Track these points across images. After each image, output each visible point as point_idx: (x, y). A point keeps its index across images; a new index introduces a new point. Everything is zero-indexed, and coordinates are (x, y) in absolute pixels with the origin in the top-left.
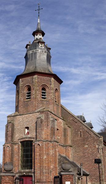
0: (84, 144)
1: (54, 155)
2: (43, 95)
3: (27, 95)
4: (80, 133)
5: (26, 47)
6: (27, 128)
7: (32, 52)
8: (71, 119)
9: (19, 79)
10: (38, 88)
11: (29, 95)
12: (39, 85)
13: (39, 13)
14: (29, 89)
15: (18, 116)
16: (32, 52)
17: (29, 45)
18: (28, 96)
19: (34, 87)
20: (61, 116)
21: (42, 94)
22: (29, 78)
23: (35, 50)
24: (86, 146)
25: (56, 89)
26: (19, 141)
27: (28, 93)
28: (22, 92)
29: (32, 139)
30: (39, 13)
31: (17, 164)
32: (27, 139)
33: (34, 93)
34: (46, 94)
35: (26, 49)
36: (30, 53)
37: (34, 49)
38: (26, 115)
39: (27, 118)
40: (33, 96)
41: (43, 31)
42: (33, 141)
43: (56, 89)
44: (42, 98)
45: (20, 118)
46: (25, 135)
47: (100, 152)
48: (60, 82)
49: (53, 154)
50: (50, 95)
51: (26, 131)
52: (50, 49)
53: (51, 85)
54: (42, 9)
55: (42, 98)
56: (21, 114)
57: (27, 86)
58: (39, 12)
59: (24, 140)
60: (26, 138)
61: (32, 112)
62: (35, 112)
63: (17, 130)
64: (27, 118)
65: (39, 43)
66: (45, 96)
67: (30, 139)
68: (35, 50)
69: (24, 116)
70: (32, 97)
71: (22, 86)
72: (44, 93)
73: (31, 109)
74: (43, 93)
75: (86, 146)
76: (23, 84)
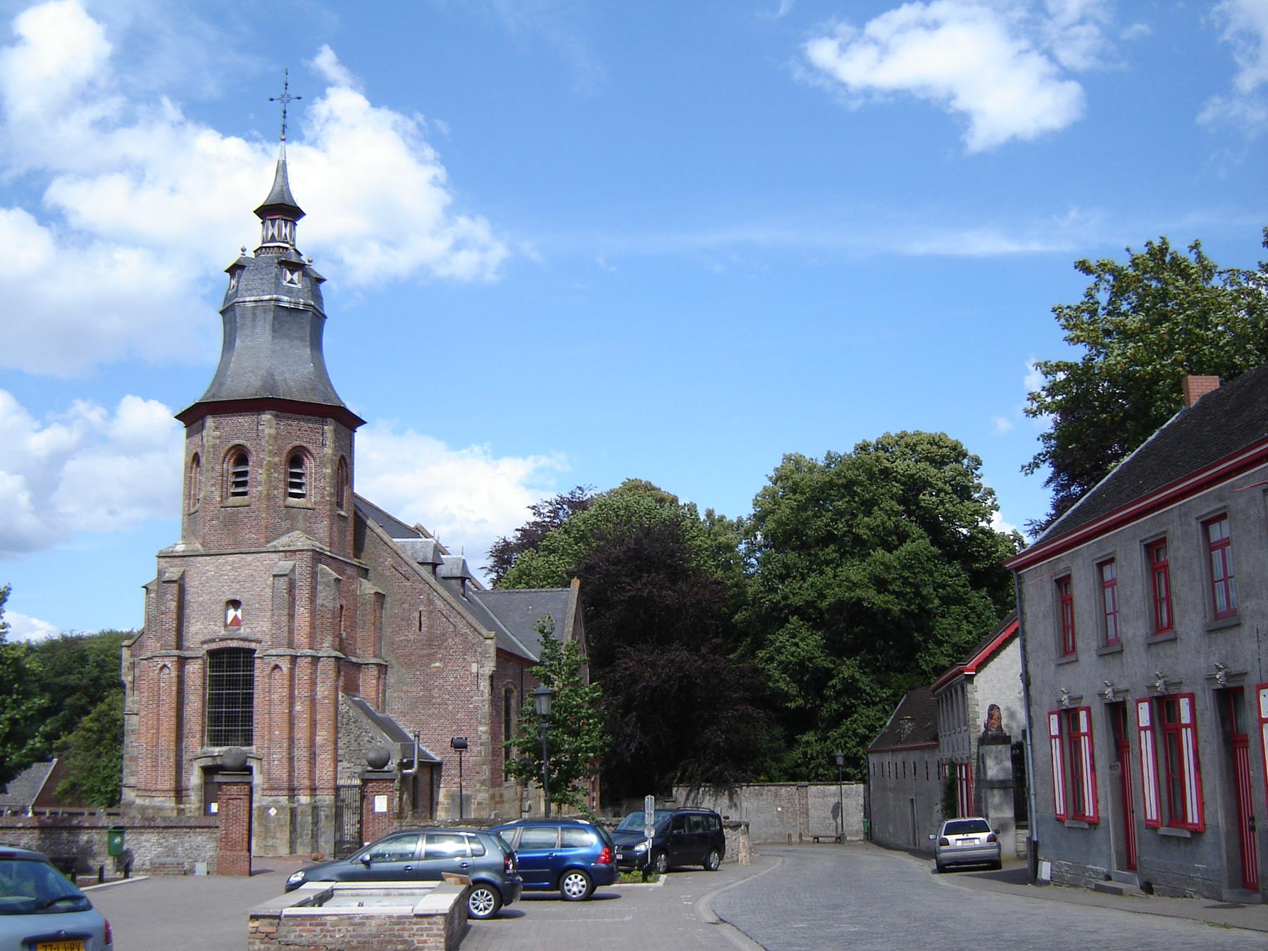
0: (431, 657)
2: (293, 485)
3: (233, 479)
6: (235, 604)
10: (276, 459)
11: (241, 481)
12: (280, 449)
22: (244, 421)
24: (437, 664)
26: (205, 646)
27: (238, 474)
29: (253, 645)
31: (198, 728)
34: (304, 480)
38: (230, 558)
40: (260, 488)
42: (254, 651)
46: (226, 626)
49: (324, 698)
50: (317, 475)
51: (232, 613)
52: (321, 280)
56: (212, 552)
61: (253, 549)
63: (195, 605)
66: (299, 486)
67: (246, 645)
69: (222, 559)
71: (214, 446)
72: (299, 476)
73: (249, 535)
75: (437, 664)
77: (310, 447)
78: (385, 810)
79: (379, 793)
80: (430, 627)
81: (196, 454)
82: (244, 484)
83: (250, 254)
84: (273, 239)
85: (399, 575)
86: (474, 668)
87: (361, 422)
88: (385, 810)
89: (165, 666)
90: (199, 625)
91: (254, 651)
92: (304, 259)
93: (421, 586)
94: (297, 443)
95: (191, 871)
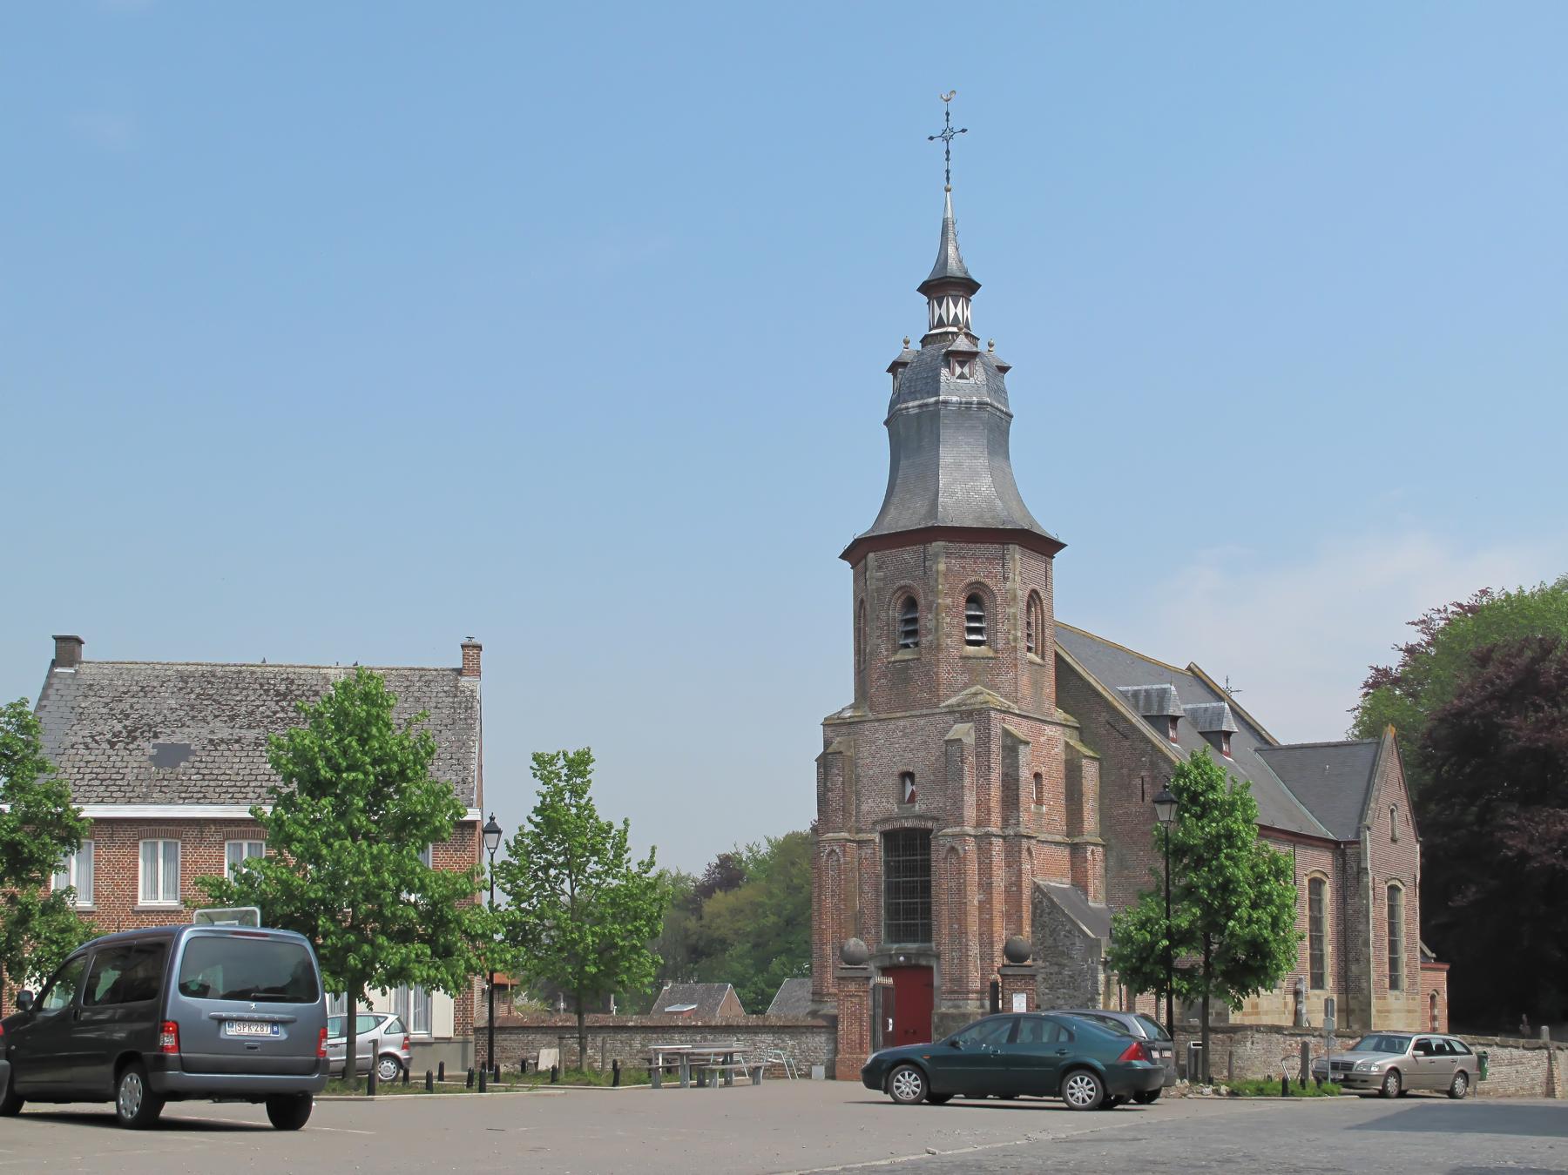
2: (971, 630)
3: (902, 628)
7: (920, 406)
14: (911, 604)
15: (867, 725)
17: (904, 364)
18: (908, 634)
22: (908, 555)
23: (933, 400)
25: (1034, 591)
26: (878, 828)
27: (907, 622)
28: (883, 615)
29: (929, 825)
31: (872, 922)
32: (908, 824)
33: (931, 625)
36: (912, 411)
37: (930, 395)
38: (902, 723)
40: (930, 638)
44: (971, 643)
52: (1004, 369)
53: (1006, 579)
54: (964, 131)
55: (971, 643)
57: (900, 588)
58: (948, 152)
59: (897, 825)
68: (933, 400)
71: (878, 590)
74: (970, 618)
78: (1024, 1010)
79: (1015, 991)
82: (914, 633)
84: (941, 323)
88: (1024, 1010)
91: (931, 831)
92: (982, 347)
93: (1142, 745)
94: (973, 579)
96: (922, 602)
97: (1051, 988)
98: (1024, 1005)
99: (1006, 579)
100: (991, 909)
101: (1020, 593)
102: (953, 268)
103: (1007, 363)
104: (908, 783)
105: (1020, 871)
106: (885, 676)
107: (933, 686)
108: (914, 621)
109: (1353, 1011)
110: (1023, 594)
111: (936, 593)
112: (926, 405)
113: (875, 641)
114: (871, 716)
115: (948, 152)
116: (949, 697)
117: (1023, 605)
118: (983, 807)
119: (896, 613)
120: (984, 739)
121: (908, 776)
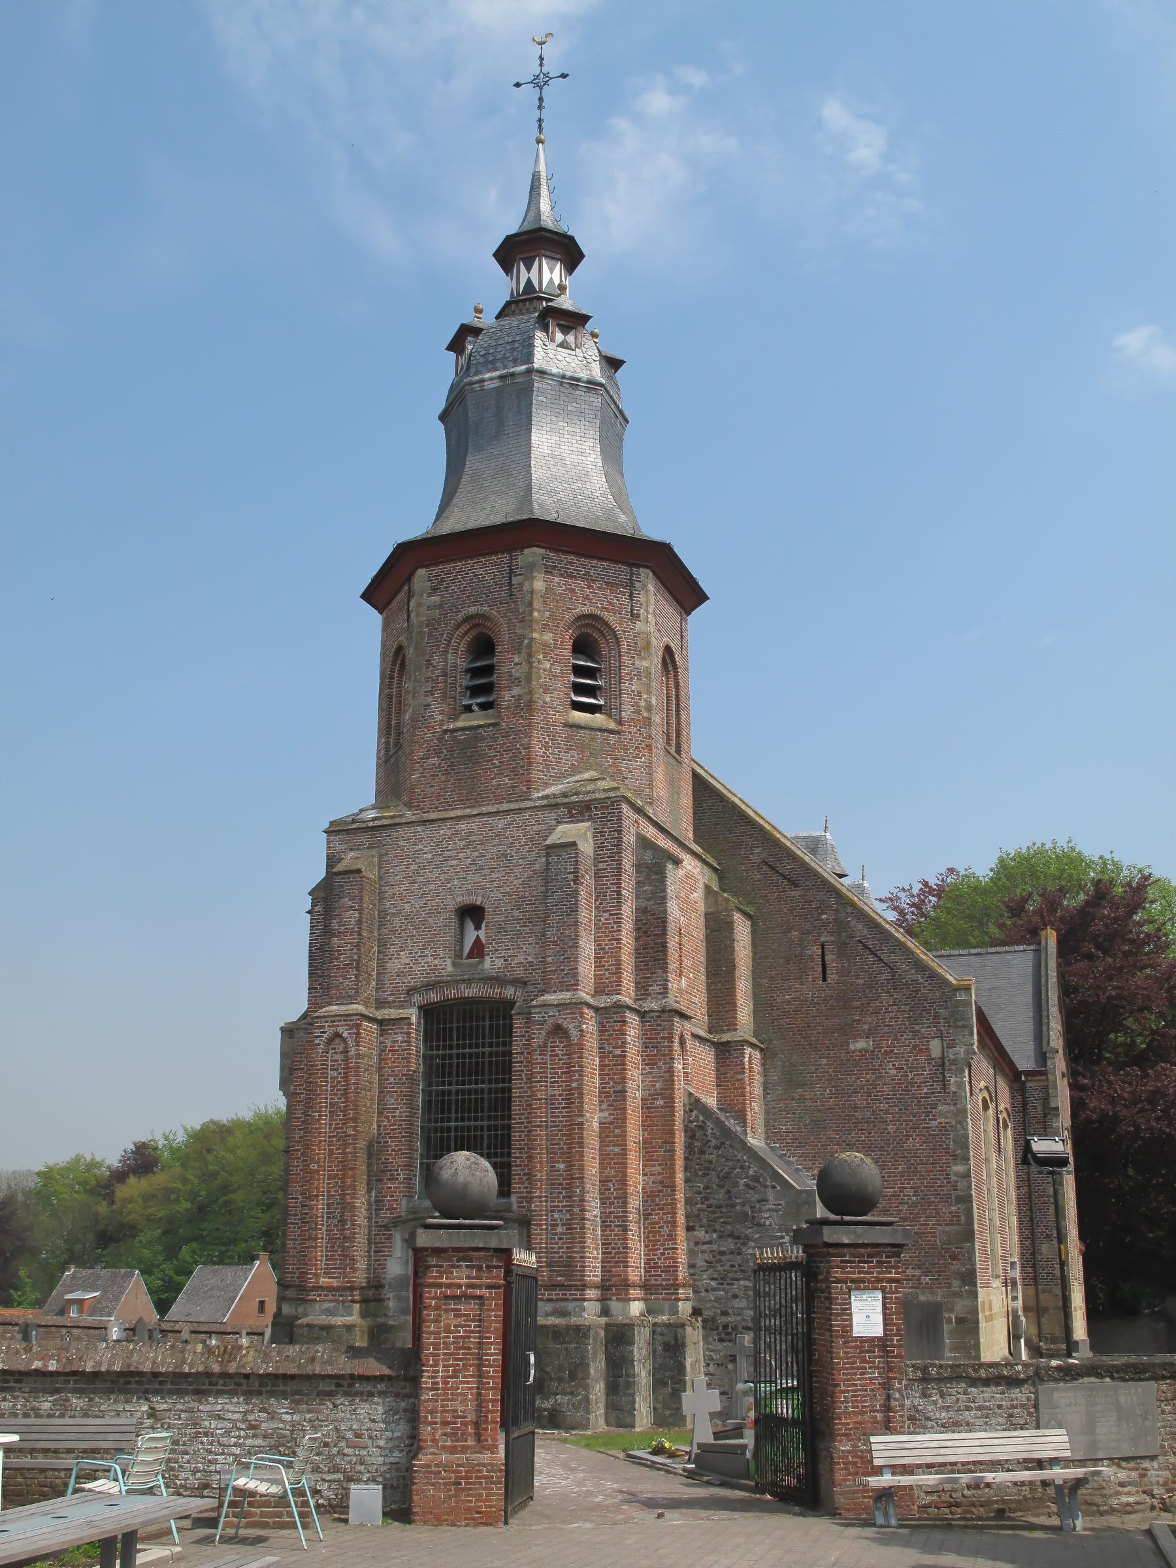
0: (849, 1031)
1: (660, 1103)
2: (579, 689)
3: (466, 681)
4: (818, 959)
5: (456, 345)
7: (501, 377)
8: (758, 854)
9: (413, 573)
13: (540, 107)
14: (484, 646)
15: (403, 832)
16: (497, 384)
18: (475, 691)
19: (519, 632)
20: (691, 835)
21: (572, 678)
22: (484, 570)
23: (523, 368)
24: (861, 1044)
26: (416, 999)
28: (437, 660)
29: (509, 992)
30: (540, 107)
31: (402, 1160)
32: (472, 992)
35: (453, 355)
36: (489, 385)
37: (515, 362)
38: (463, 826)
39: (469, 844)
40: (516, 691)
41: (572, 239)
43: (668, 649)
44: (578, 706)
45: (420, 844)
47: (953, 1089)
48: (686, 593)
53: (635, 617)
58: (541, 99)
59: (450, 993)
60: (468, 982)
62: (528, 804)
64: (469, 844)
65: (552, 324)
66: (590, 691)
67: (495, 992)
68: (523, 368)
70: (506, 695)
72: (590, 673)
74: (578, 671)
75: (861, 1044)
76: (440, 606)
77: (607, 616)
78: (878, 1331)
79: (859, 1284)
80: (843, 973)
81: (400, 649)
83: (487, 320)
85: (777, 879)
86: (935, 1047)
87: (701, 597)
88: (878, 1331)
89: (338, 1035)
90: (404, 957)
91: (511, 1004)
93: (821, 895)
94: (586, 610)
95: (337, 1509)
96: (503, 640)
97: (722, 1279)
98: (857, 1319)
99: (635, 617)
100: (623, 1136)
101: (654, 641)
102: (547, 219)
103: (618, 356)
104: (470, 926)
105: (671, 1071)
106: (438, 752)
107: (520, 767)
108: (489, 670)
109: (1046, 1310)
110: (657, 644)
111: (526, 620)
112: (513, 375)
113: (422, 700)
114: (409, 815)
115: (541, 99)
116: (547, 785)
117: (658, 660)
118: (606, 958)
119: (458, 658)
120: (610, 846)
121: (472, 913)
